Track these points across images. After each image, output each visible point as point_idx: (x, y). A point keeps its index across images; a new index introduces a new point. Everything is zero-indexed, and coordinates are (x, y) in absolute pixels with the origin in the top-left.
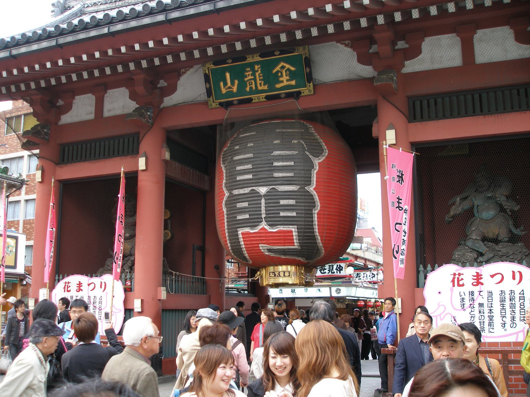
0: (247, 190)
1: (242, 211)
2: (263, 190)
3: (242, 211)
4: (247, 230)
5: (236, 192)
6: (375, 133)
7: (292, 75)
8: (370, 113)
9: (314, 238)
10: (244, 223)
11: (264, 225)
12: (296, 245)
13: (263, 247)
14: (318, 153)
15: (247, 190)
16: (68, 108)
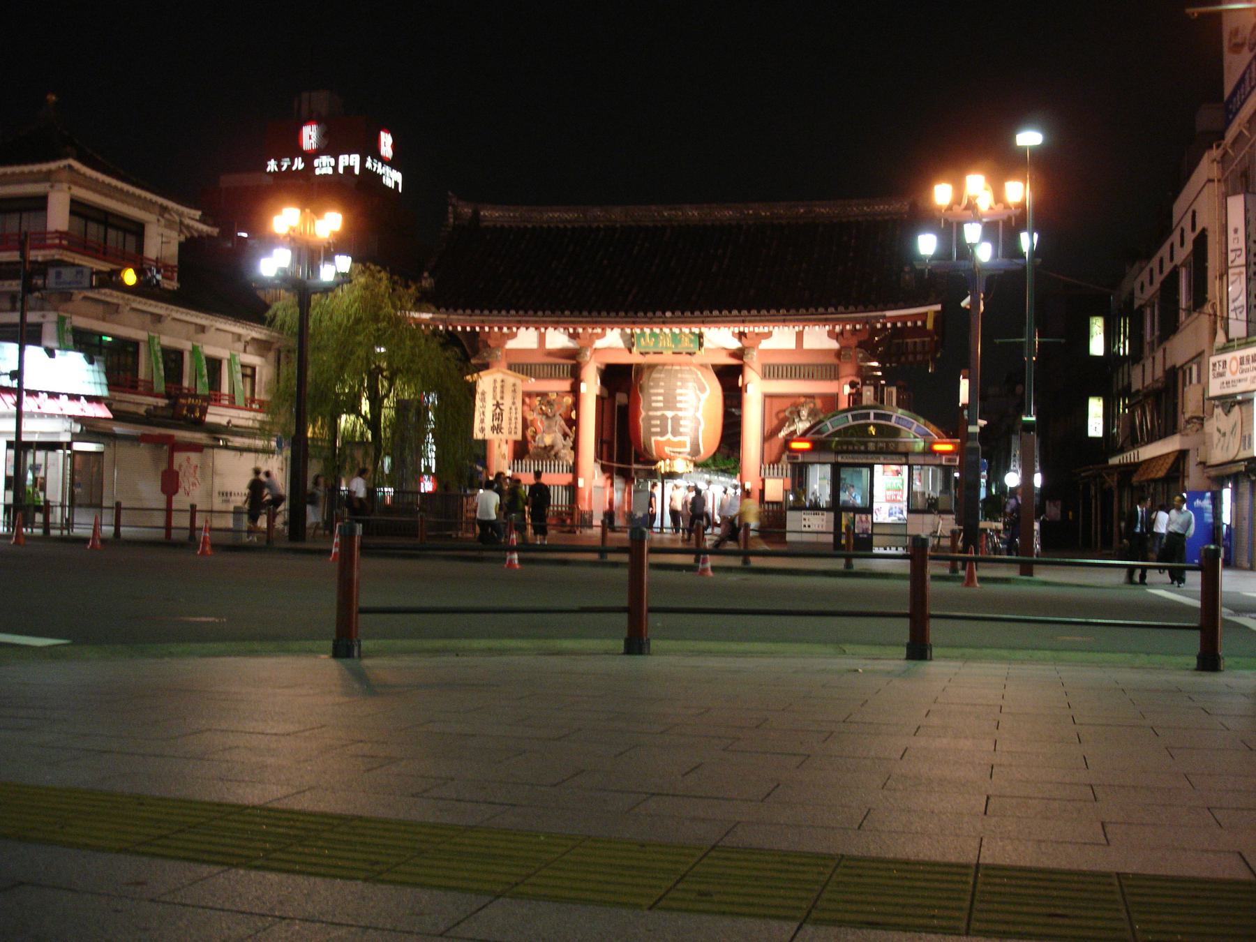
0: (659, 413)
1: (656, 426)
2: (669, 414)
3: (656, 426)
4: (659, 438)
5: (651, 413)
6: (740, 384)
7: (691, 341)
8: (738, 370)
9: (698, 445)
10: (656, 434)
11: (669, 436)
12: (688, 449)
13: (667, 450)
14: (702, 389)
15: (659, 413)
16: (514, 336)
